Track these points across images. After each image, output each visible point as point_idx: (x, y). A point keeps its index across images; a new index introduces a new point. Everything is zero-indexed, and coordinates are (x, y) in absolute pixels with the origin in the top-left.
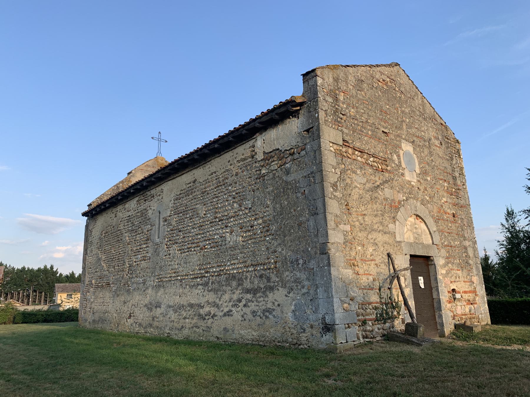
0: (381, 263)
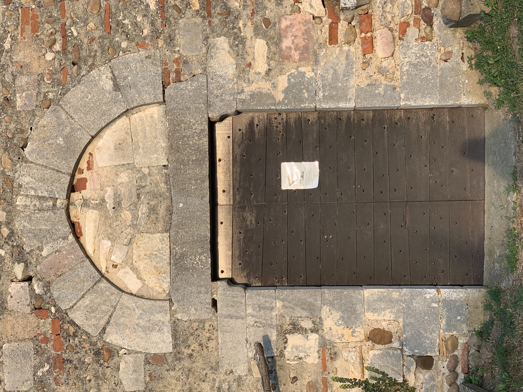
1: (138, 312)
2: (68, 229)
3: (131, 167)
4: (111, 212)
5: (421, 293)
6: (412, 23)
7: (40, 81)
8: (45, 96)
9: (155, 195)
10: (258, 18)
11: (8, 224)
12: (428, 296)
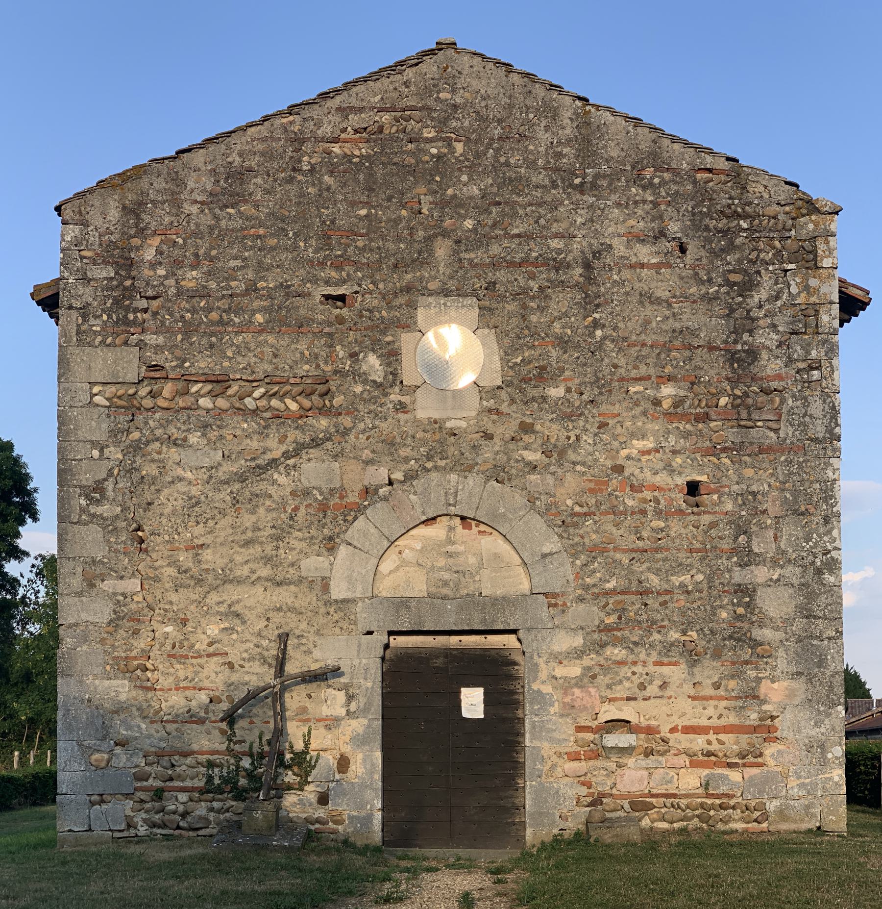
0: (251, 659)
1: (364, 571)
2: (431, 515)
3: (481, 566)
4: (445, 550)
5: (378, 796)
6: (591, 791)
7: (549, 494)
8: (537, 498)
9: (457, 586)
10: (597, 669)
11: (436, 467)
12: (375, 802)
